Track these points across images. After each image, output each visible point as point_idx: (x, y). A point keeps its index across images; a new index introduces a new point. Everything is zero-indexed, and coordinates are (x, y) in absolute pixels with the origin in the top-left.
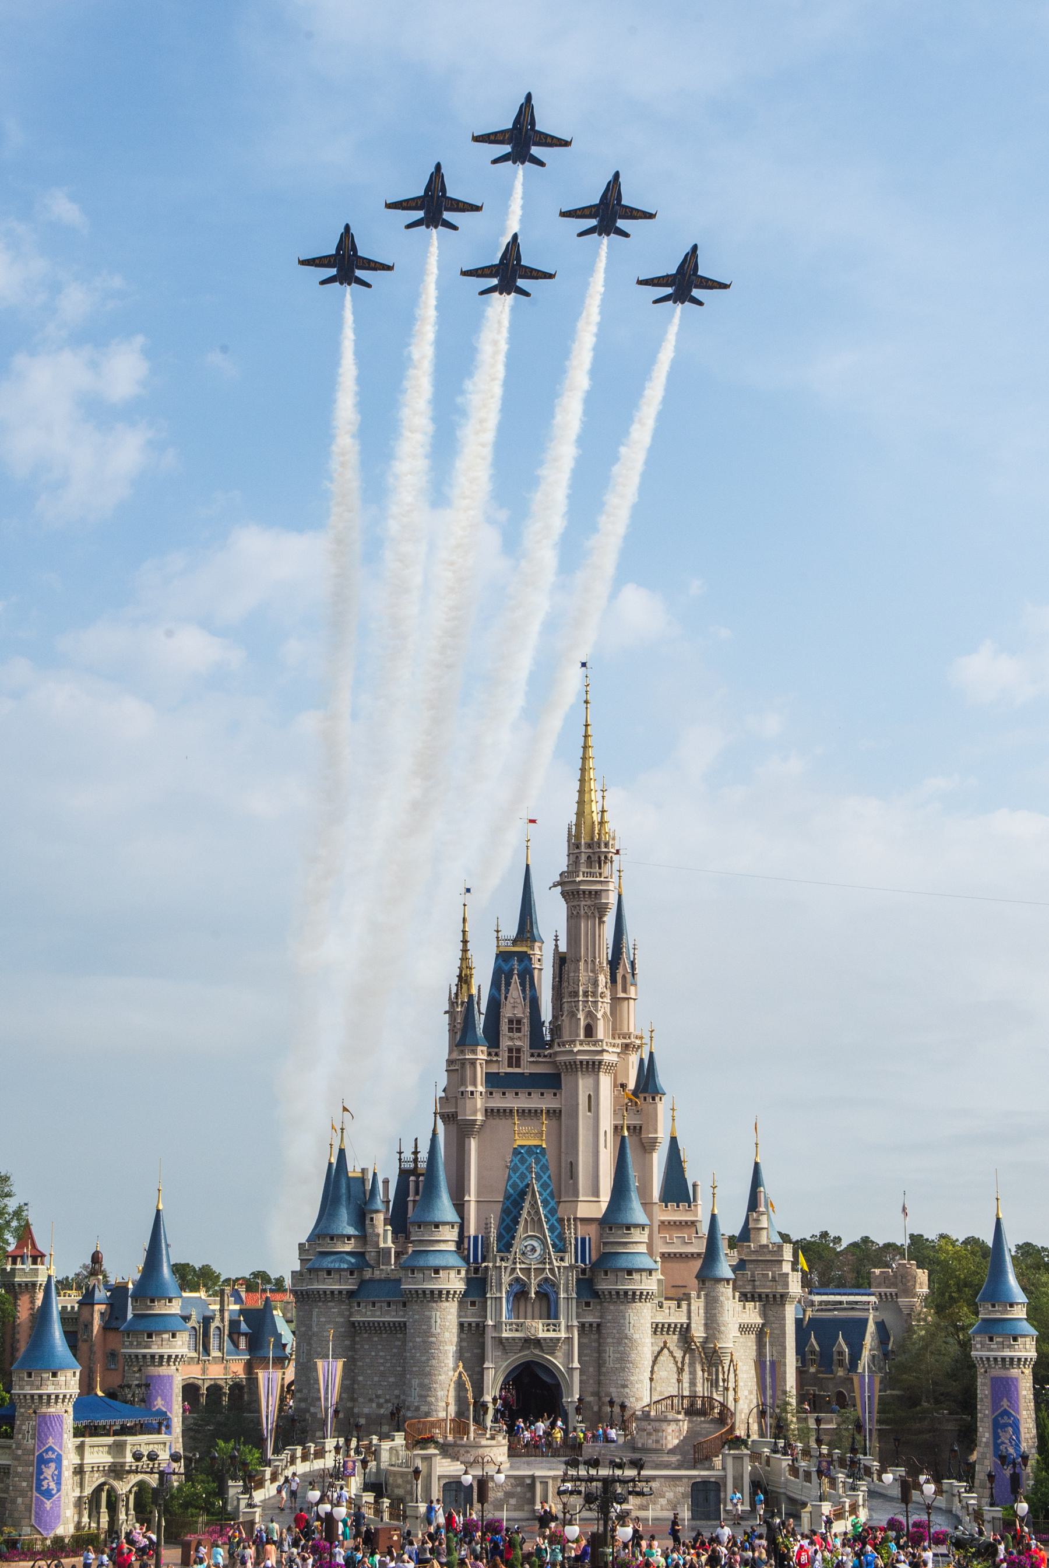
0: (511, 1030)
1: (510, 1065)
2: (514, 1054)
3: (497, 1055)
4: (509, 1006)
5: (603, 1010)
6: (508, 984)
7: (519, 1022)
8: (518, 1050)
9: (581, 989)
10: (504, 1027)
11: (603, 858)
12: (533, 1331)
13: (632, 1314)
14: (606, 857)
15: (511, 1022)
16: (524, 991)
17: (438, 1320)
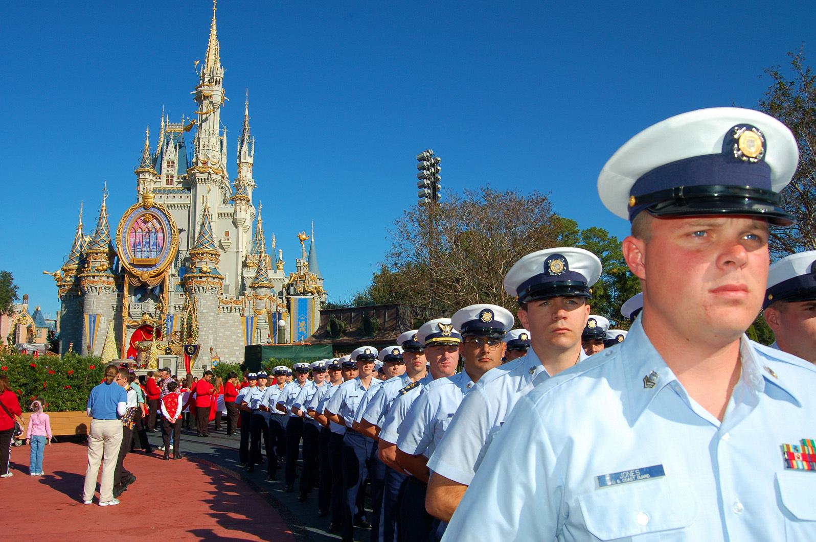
0: (168, 166)
1: (167, 184)
2: (169, 178)
3: (160, 179)
4: (168, 155)
5: (213, 154)
6: (168, 144)
7: (173, 162)
8: (172, 177)
9: (201, 143)
10: (165, 165)
11: (215, 79)
12: (146, 308)
13: (202, 300)
14: (216, 79)
15: (168, 162)
16: (175, 148)
17: (95, 303)
